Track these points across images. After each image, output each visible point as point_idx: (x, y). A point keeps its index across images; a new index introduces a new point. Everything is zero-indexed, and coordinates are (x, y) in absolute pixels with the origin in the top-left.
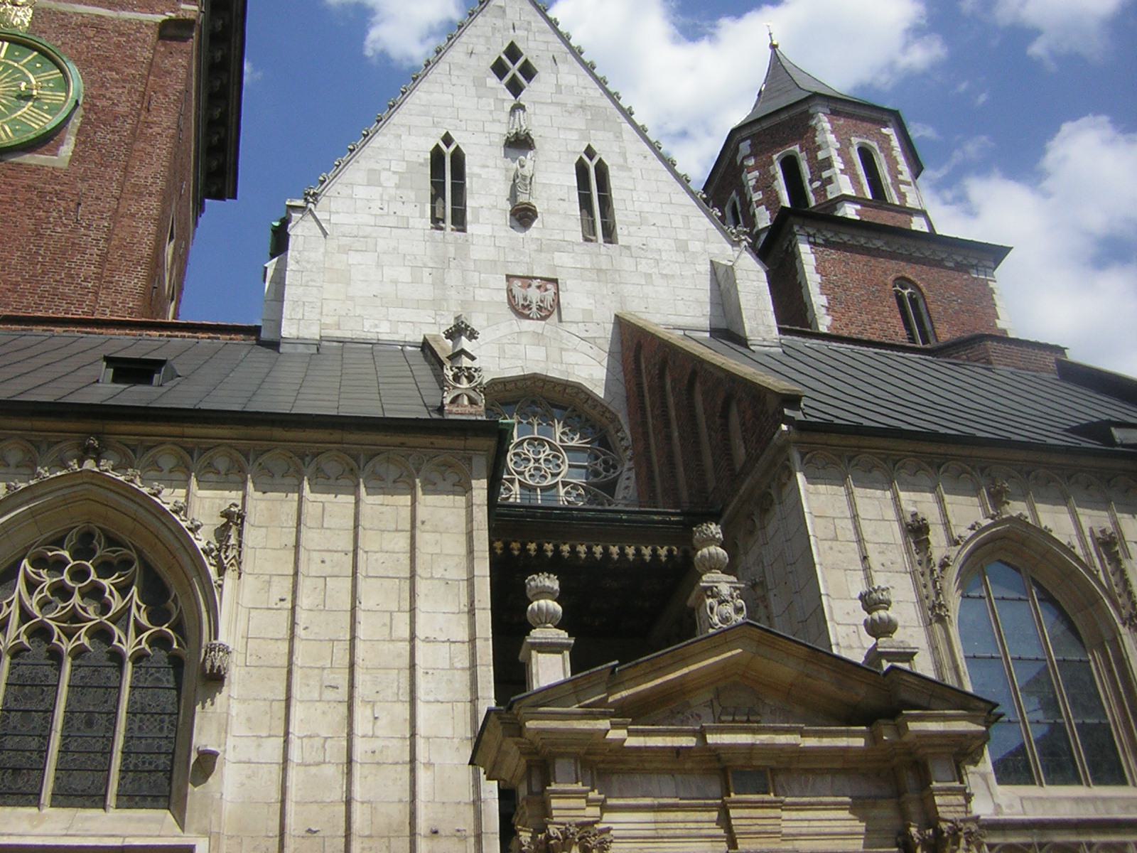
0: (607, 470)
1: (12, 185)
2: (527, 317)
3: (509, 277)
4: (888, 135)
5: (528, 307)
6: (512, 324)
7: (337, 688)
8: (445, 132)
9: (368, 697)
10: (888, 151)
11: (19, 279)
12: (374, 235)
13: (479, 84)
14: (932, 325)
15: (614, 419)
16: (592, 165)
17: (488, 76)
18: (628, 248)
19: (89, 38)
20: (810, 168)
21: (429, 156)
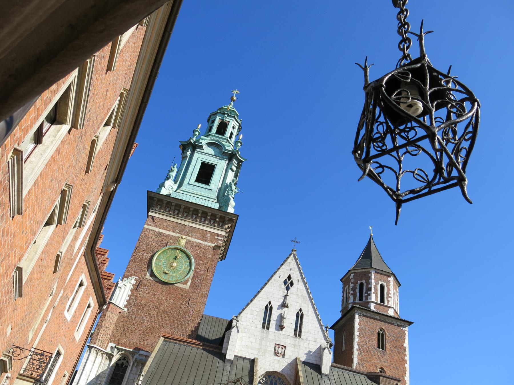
1: (176, 293)
2: (277, 356)
3: (276, 344)
4: (390, 281)
5: (278, 353)
8: (269, 301)
10: (388, 286)
11: (175, 319)
12: (249, 329)
13: (280, 286)
14: (386, 344)
16: (300, 314)
18: (303, 339)
19: (197, 250)
20: (366, 289)
21: (265, 307)
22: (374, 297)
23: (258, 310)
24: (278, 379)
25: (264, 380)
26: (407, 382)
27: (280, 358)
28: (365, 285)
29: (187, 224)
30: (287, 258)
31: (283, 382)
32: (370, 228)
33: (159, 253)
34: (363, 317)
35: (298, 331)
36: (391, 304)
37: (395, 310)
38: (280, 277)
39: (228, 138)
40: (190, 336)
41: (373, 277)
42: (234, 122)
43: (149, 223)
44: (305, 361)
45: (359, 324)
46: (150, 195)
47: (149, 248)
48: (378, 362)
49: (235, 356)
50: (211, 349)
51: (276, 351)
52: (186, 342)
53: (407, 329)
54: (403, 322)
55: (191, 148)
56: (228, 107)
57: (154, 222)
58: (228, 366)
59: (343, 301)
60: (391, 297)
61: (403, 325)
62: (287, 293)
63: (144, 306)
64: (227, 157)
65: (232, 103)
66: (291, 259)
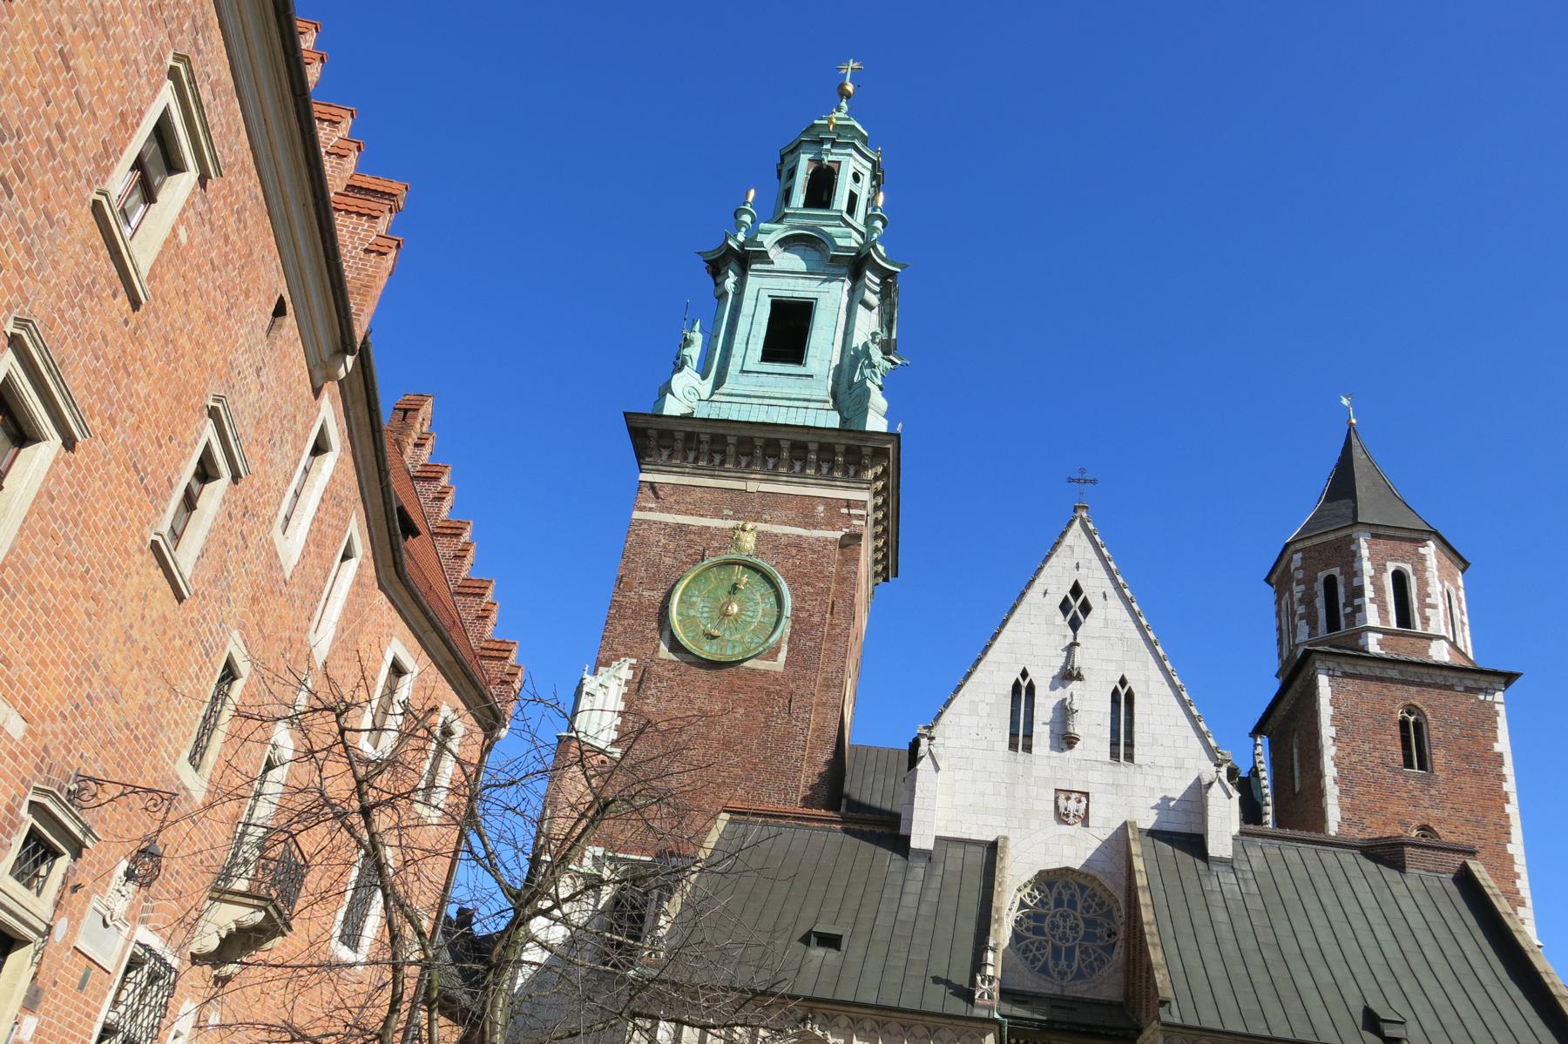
0: (1109, 936)
2: (1067, 823)
5: (1067, 816)
10: (1420, 571)
13: (1050, 622)
15: (1117, 901)
16: (1123, 692)
18: (1140, 766)
19: (793, 557)
20: (1346, 592)
21: (1011, 689)
22: (1376, 614)
23: (990, 699)
25: (1035, 898)
26: (1516, 861)
27: (1077, 828)
28: (1341, 581)
29: (752, 486)
30: (1063, 534)
31: (1095, 895)
32: (1345, 402)
33: (686, 582)
34: (1345, 680)
35: (1122, 744)
36: (1438, 625)
37: (1453, 645)
38: (1045, 593)
39: (841, 211)
40: (808, 802)
41: (1365, 552)
42: (855, 160)
43: (643, 504)
44: (1155, 828)
45: (1334, 703)
47: (654, 575)
48: (1411, 808)
49: (938, 839)
50: (866, 828)
51: (1062, 810)
52: (795, 818)
53: (1499, 696)
54: (1483, 678)
55: (733, 265)
56: (830, 120)
57: (658, 498)
58: (919, 870)
59: (1280, 642)
60: (1434, 607)
61: (1484, 685)
62: (1075, 638)
64: (844, 271)
65: (844, 104)
66: (1075, 536)
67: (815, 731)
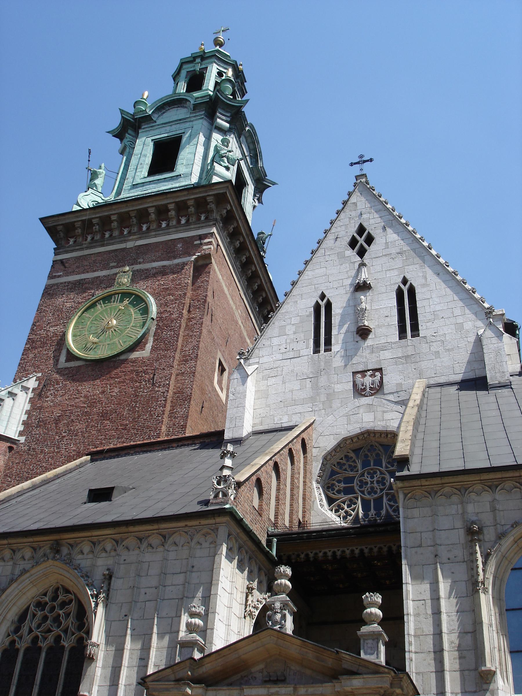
1: (124, 372)
2: (365, 396)
3: (354, 373)
5: (364, 390)
6: (355, 402)
7: (144, 659)
9: (157, 664)
12: (282, 365)
13: (341, 256)
16: (405, 289)
17: (346, 250)
18: (425, 337)
24: (382, 450)
43: (54, 274)
46: (47, 226)
47: (58, 315)
63: (57, 421)
67: (175, 393)
